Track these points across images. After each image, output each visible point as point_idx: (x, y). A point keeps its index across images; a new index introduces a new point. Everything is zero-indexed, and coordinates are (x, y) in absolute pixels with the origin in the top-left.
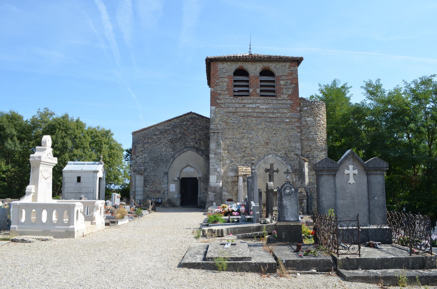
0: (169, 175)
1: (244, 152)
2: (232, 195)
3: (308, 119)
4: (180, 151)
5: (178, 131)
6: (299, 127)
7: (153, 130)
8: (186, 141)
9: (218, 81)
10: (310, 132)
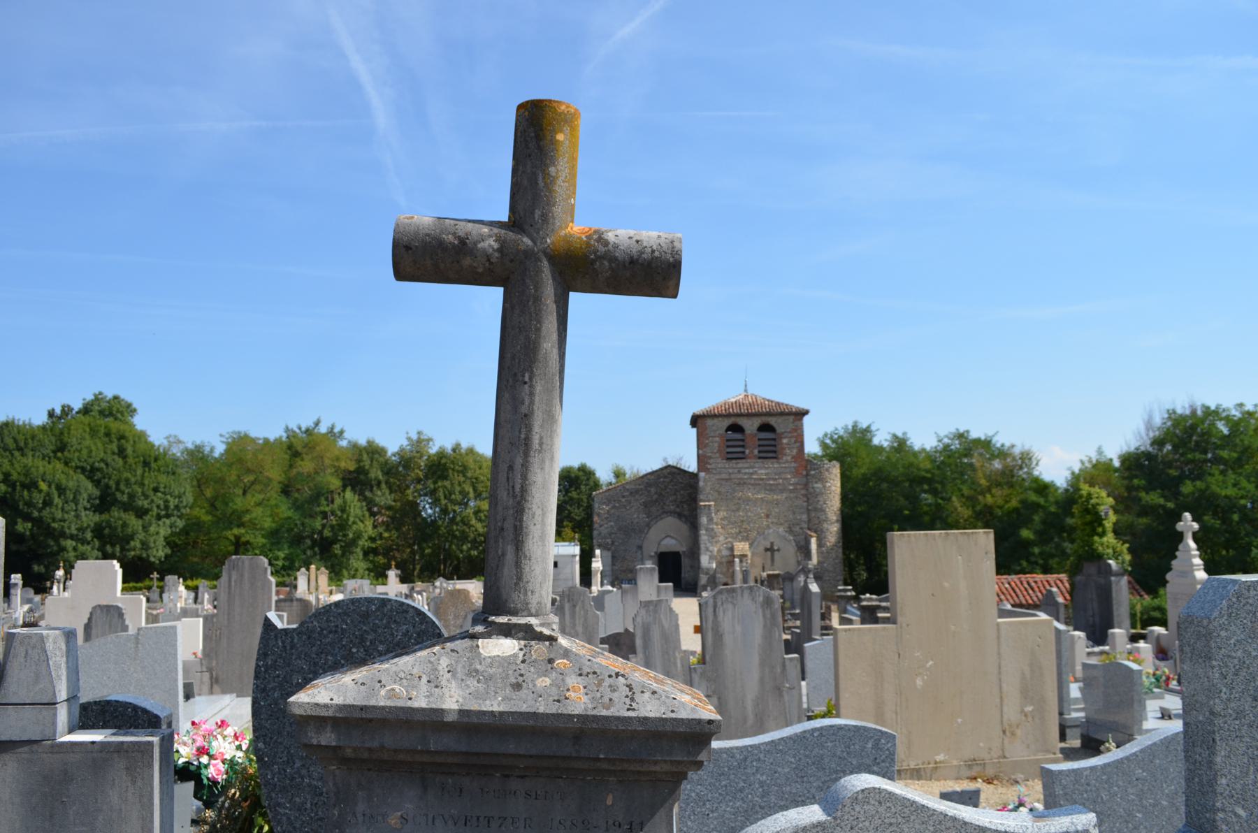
0: (644, 549)
3: (816, 485)
4: (656, 518)
5: (653, 490)
6: (805, 495)
8: (664, 504)
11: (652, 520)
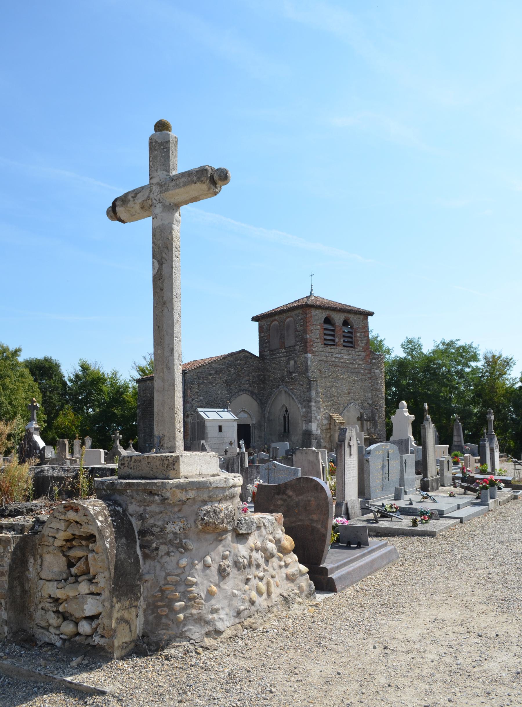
1: (333, 400)
2: (325, 442)
3: (376, 371)
4: (235, 394)
6: (370, 378)
7: (208, 368)
8: (241, 383)
9: (312, 328)
10: (378, 383)
11: (232, 396)
